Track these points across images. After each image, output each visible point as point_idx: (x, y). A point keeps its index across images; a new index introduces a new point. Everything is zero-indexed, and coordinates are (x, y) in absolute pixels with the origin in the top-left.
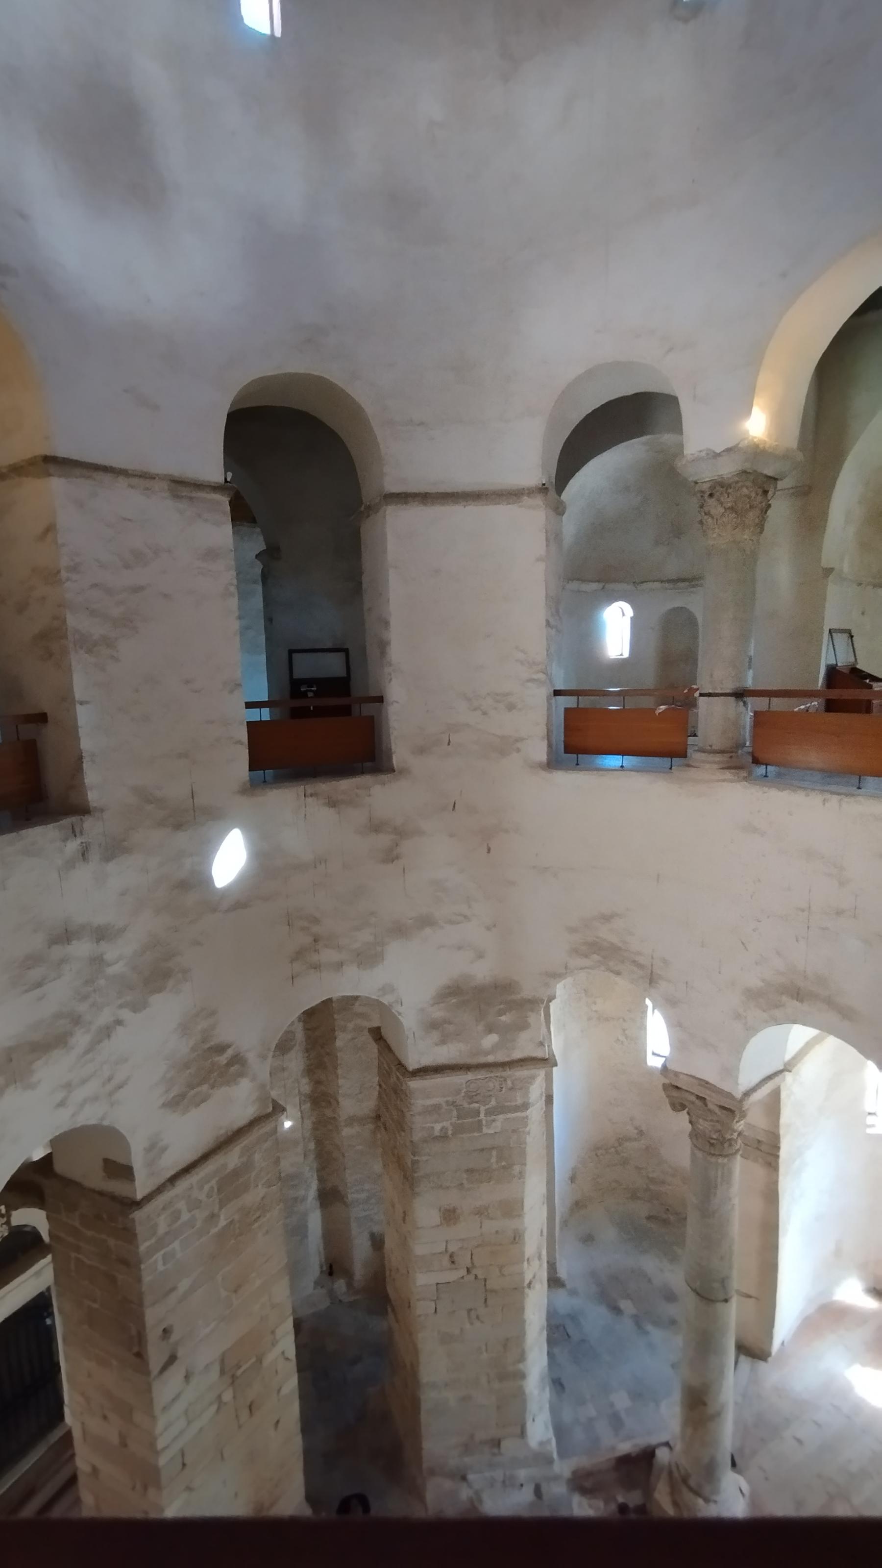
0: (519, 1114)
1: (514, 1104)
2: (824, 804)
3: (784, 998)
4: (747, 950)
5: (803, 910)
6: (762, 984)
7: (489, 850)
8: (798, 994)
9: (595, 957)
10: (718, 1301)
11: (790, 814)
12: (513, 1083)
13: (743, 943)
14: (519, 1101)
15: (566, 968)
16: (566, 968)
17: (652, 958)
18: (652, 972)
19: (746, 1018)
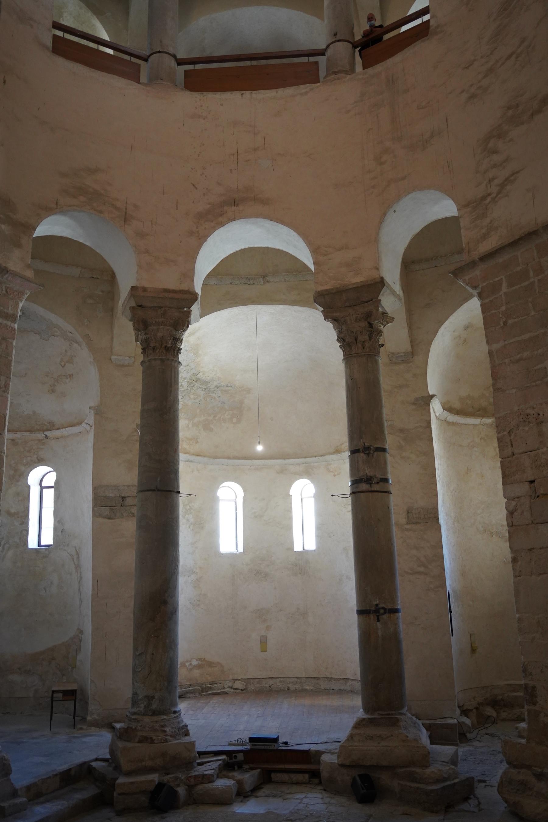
0: (9, 323)
1: (6, 310)
2: (242, 96)
3: (225, 208)
4: (197, 189)
5: (234, 154)
6: (209, 206)
7: (4, 82)
8: (235, 203)
9: (82, 199)
10: (174, 492)
11: (222, 105)
12: (7, 291)
13: (193, 185)
14: (10, 311)
15: (57, 204)
16: (57, 204)
17: (126, 203)
18: (126, 213)
19: (198, 232)
